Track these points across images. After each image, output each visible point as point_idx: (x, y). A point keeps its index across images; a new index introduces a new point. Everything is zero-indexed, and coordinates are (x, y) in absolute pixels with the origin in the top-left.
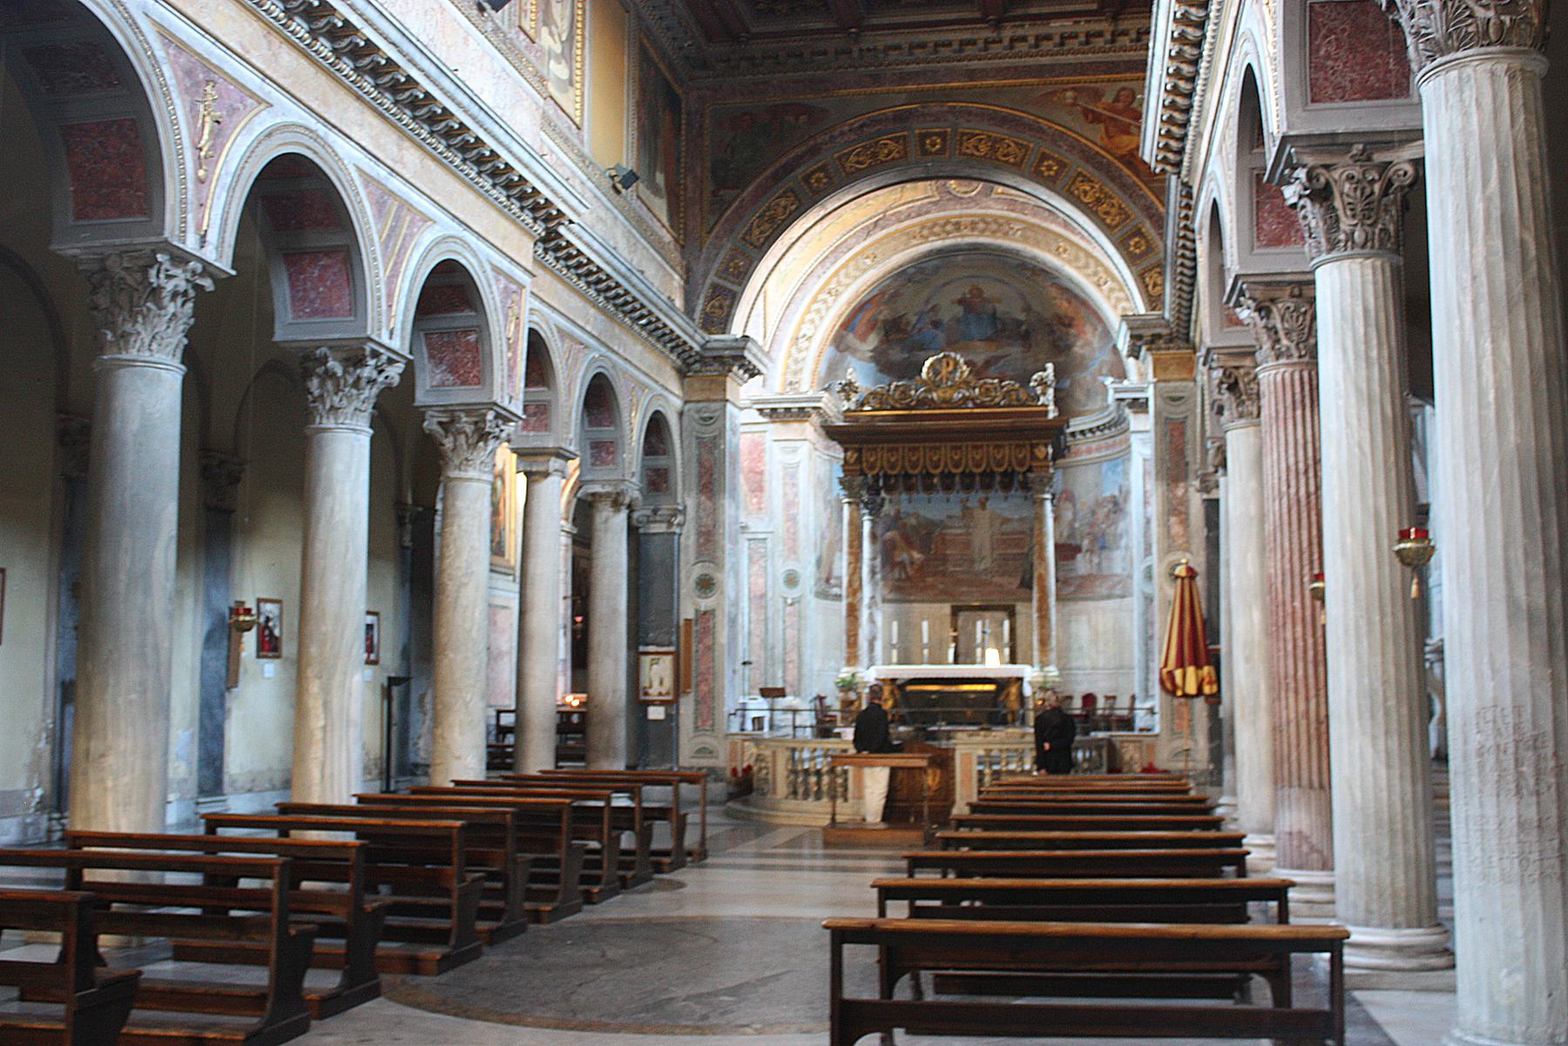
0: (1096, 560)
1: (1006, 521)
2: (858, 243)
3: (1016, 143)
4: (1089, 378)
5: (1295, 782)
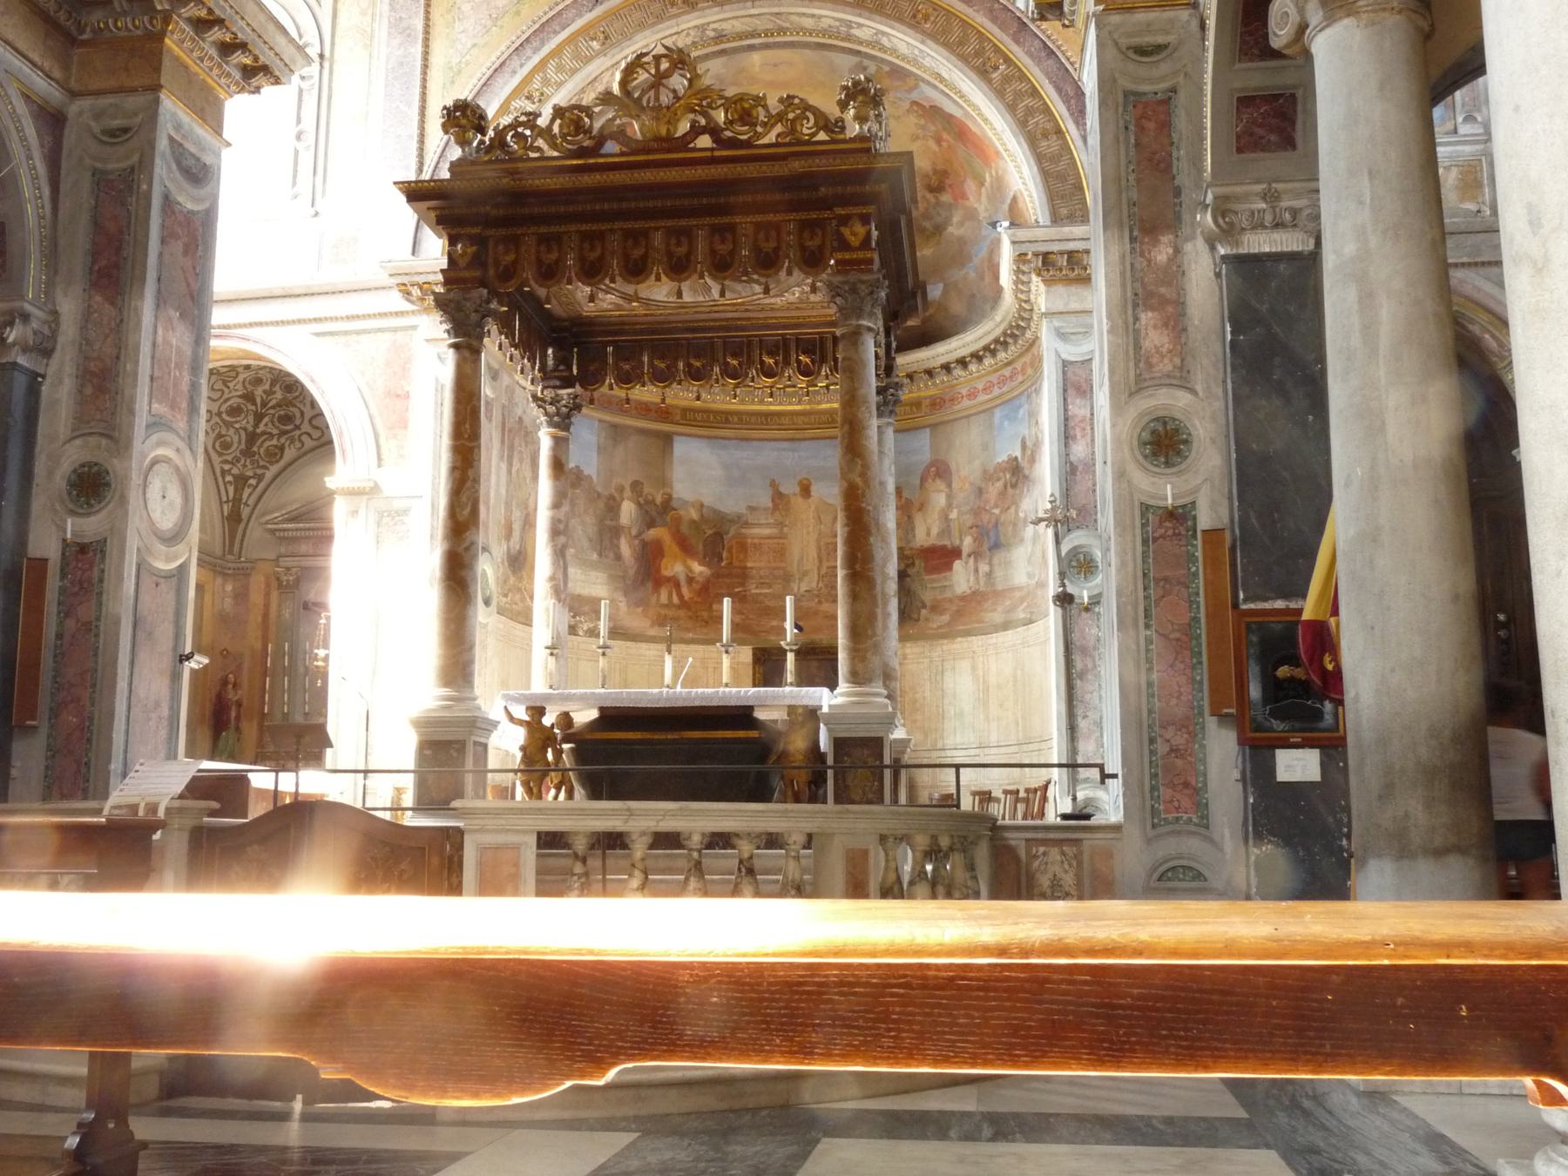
2: (580, 15)
4: (972, 275)
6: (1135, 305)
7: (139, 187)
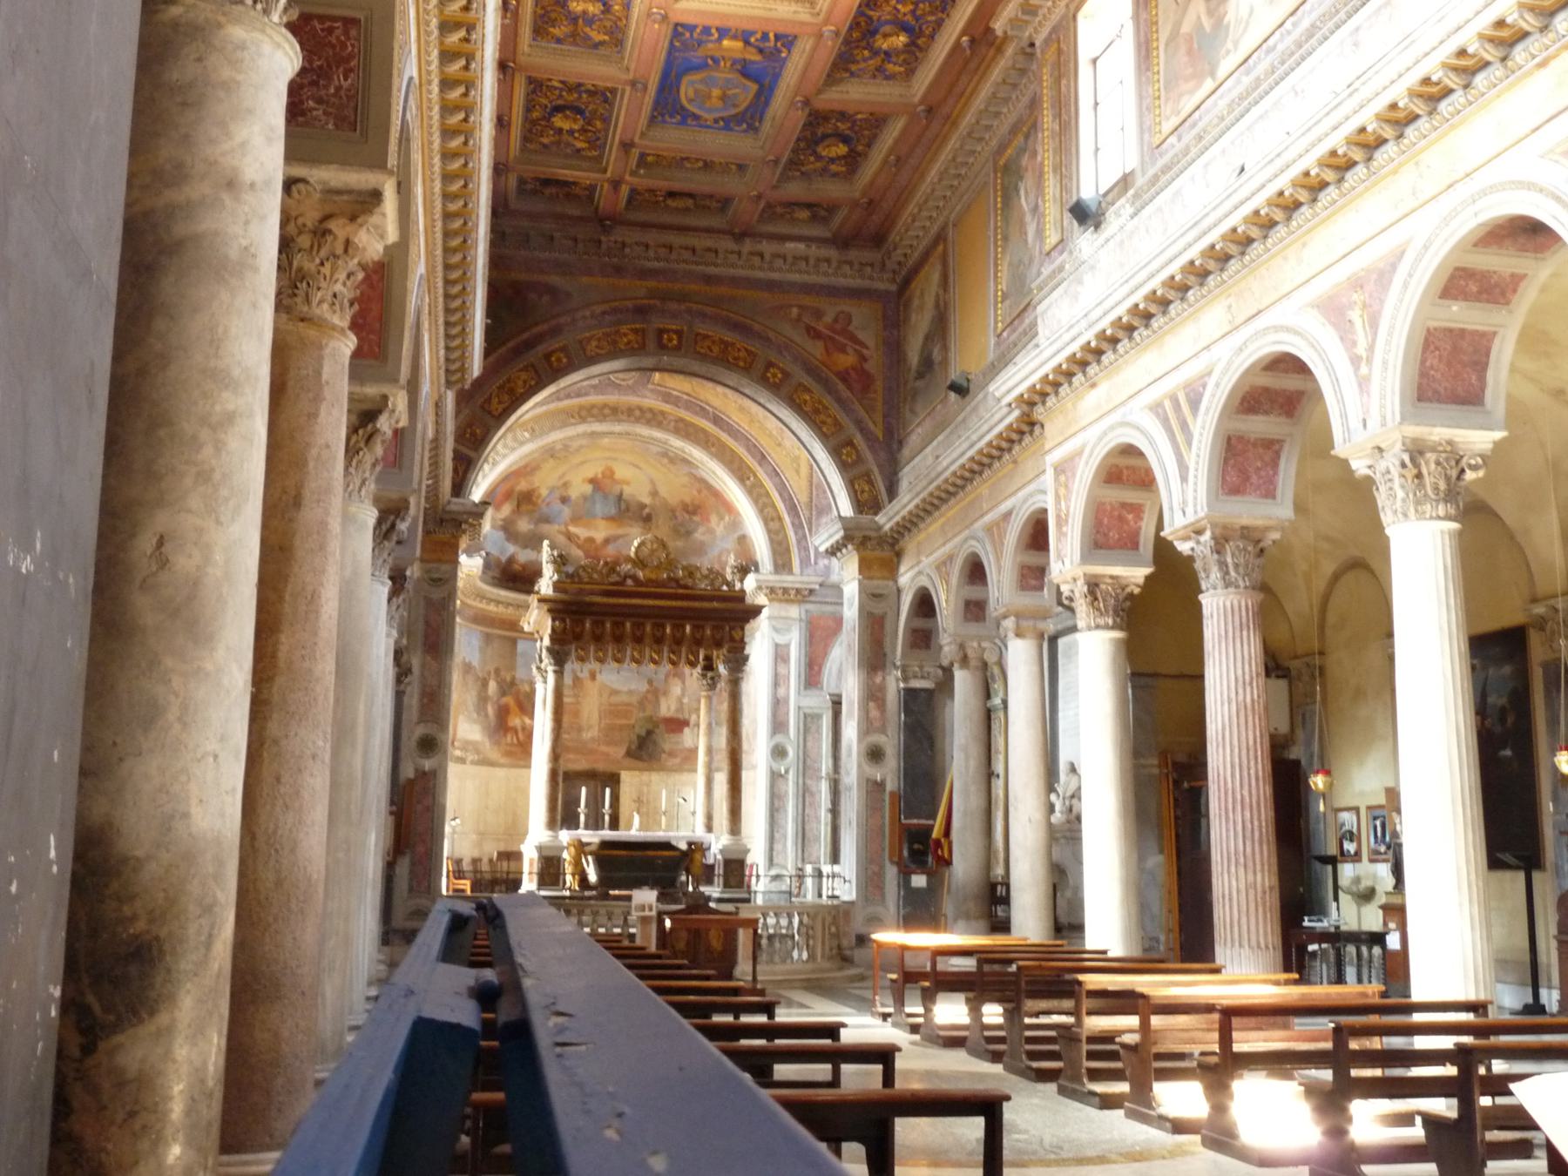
1: (615, 692)
3: (746, 350)
5: (1245, 943)
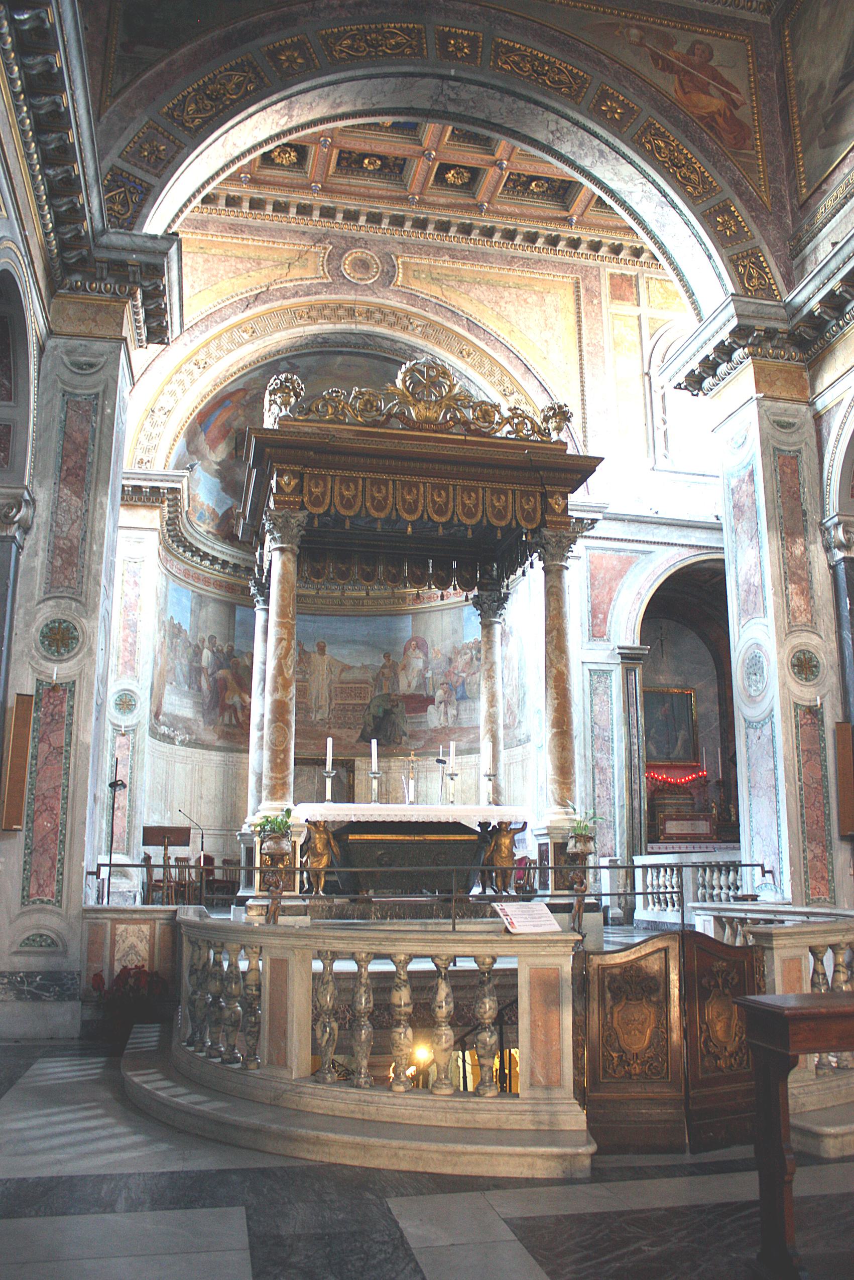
0: (452, 711)
1: (347, 668)
6: (786, 580)
7: (103, 409)
